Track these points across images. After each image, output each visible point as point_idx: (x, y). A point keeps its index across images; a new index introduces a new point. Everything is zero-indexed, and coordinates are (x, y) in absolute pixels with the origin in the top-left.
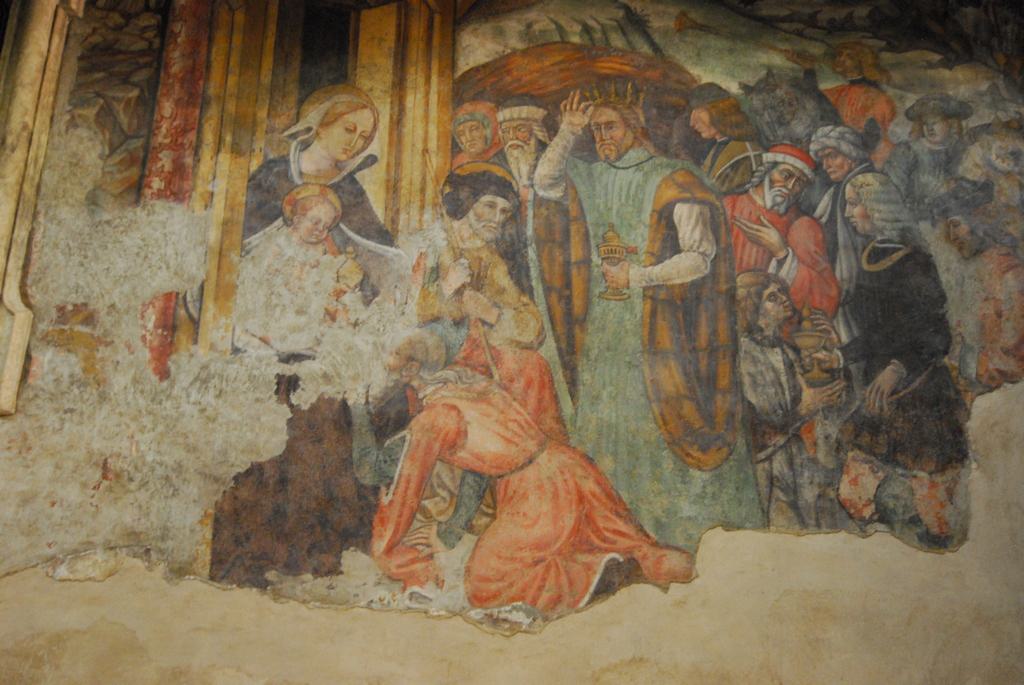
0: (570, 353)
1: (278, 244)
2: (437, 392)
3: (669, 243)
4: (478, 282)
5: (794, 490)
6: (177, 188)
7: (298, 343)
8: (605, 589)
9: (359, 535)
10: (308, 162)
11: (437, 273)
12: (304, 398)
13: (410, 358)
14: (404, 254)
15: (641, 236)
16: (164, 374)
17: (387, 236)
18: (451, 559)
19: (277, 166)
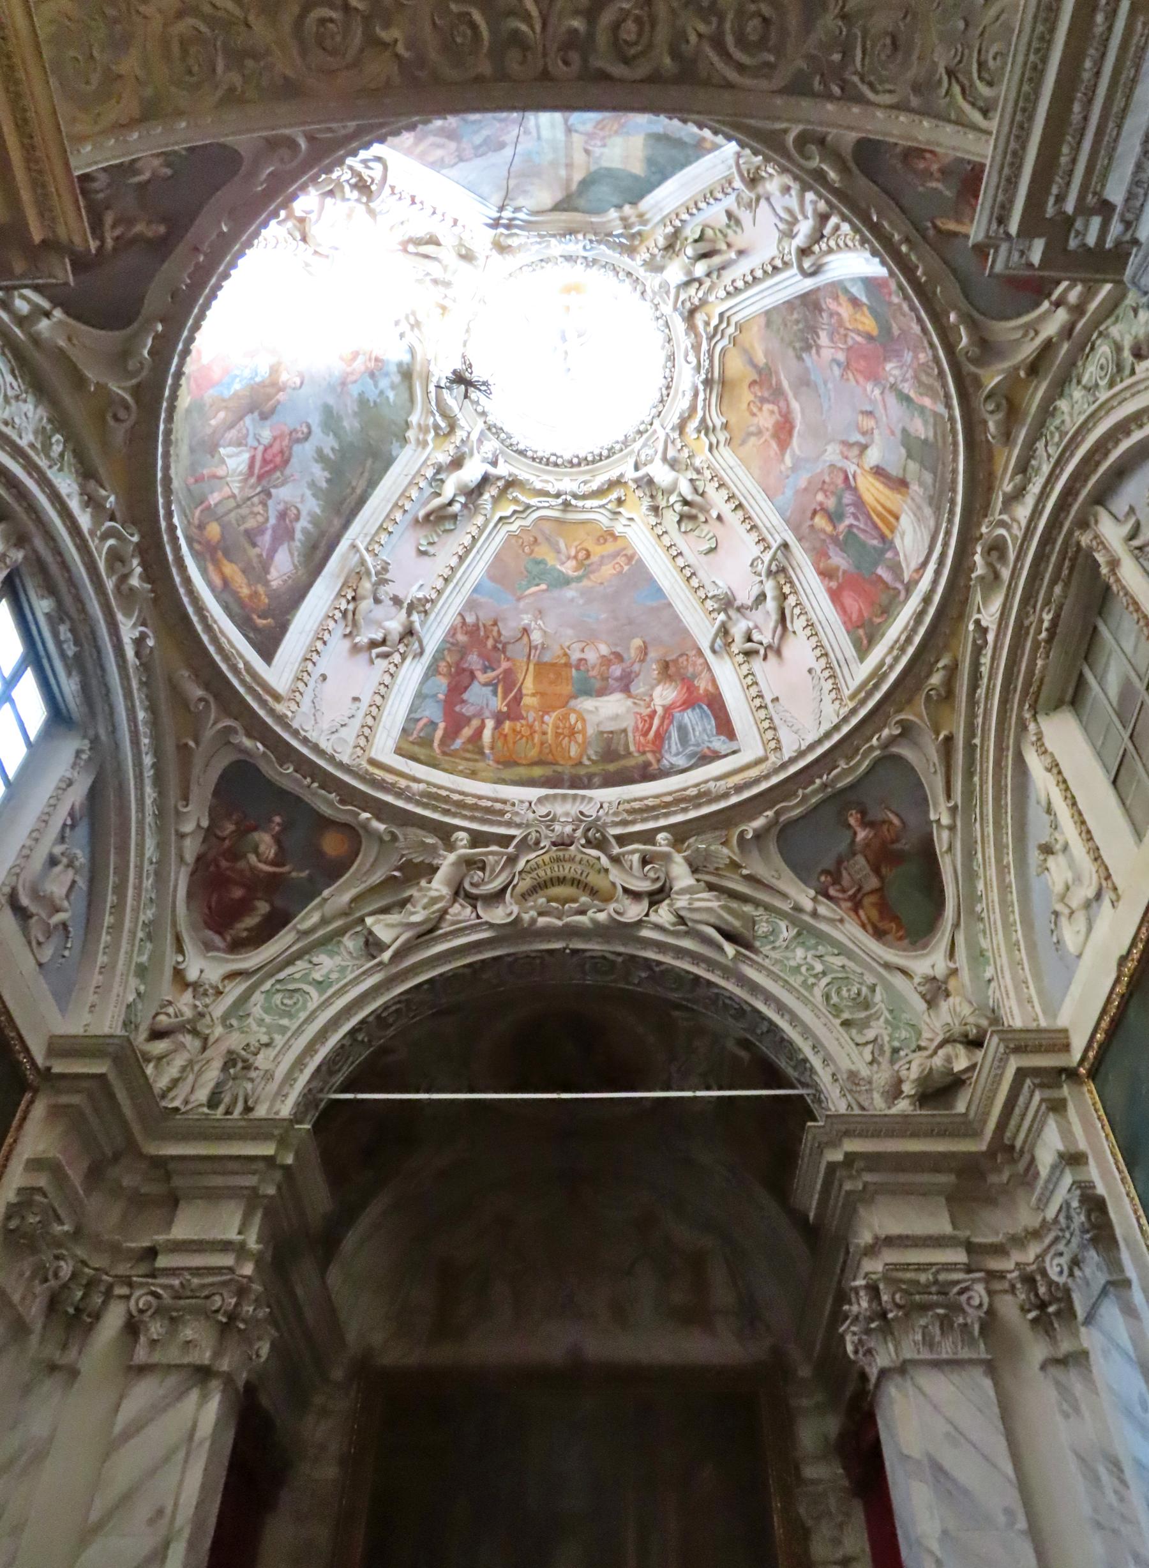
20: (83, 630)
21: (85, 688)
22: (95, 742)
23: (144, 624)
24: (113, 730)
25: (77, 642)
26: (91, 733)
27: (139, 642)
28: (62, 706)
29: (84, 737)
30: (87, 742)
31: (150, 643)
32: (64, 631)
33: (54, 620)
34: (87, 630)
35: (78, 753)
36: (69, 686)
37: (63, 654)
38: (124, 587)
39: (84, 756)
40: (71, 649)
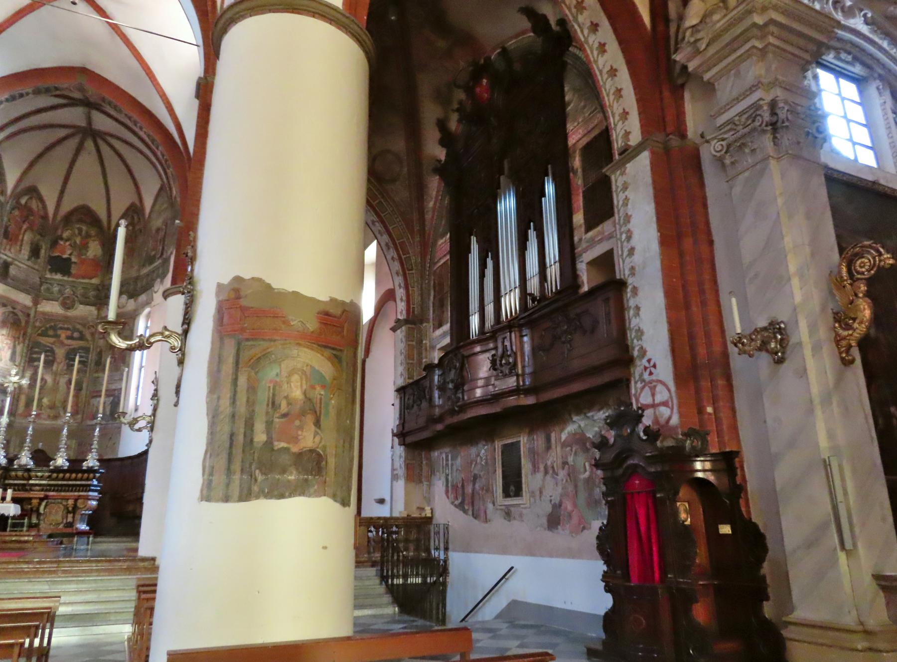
0: (576, 492)
1: (548, 477)
2: (564, 501)
3: (585, 471)
4: (567, 481)
5: (601, 513)
6: (538, 471)
7: (550, 494)
8: (582, 531)
9: (559, 524)
10: (549, 463)
11: (562, 480)
12: (553, 502)
13: (561, 496)
14: (559, 478)
15: (582, 470)
16: (541, 500)
17: (557, 475)
18: (568, 526)
19: (546, 464)
20: (848, 47)
21: (864, 64)
22: (881, 77)
23: (861, 10)
24: (883, 66)
25: (849, 53)
26: (876, 75)
27: (866, 22)
28: (856, 76)
29: (875, 79)
30: (878, 81)
31: (869, 15)
32: (843, 56)
33: (837, 58)
34: (849, 45)
35: (878, 88)
36: (858, 69)
37: (847, 63)
38: (846, 10)
39: (881, 87)
40: (849, 58)
